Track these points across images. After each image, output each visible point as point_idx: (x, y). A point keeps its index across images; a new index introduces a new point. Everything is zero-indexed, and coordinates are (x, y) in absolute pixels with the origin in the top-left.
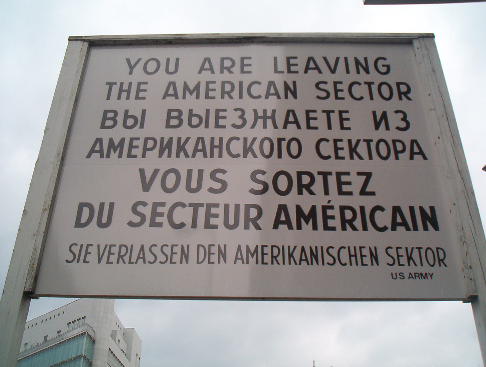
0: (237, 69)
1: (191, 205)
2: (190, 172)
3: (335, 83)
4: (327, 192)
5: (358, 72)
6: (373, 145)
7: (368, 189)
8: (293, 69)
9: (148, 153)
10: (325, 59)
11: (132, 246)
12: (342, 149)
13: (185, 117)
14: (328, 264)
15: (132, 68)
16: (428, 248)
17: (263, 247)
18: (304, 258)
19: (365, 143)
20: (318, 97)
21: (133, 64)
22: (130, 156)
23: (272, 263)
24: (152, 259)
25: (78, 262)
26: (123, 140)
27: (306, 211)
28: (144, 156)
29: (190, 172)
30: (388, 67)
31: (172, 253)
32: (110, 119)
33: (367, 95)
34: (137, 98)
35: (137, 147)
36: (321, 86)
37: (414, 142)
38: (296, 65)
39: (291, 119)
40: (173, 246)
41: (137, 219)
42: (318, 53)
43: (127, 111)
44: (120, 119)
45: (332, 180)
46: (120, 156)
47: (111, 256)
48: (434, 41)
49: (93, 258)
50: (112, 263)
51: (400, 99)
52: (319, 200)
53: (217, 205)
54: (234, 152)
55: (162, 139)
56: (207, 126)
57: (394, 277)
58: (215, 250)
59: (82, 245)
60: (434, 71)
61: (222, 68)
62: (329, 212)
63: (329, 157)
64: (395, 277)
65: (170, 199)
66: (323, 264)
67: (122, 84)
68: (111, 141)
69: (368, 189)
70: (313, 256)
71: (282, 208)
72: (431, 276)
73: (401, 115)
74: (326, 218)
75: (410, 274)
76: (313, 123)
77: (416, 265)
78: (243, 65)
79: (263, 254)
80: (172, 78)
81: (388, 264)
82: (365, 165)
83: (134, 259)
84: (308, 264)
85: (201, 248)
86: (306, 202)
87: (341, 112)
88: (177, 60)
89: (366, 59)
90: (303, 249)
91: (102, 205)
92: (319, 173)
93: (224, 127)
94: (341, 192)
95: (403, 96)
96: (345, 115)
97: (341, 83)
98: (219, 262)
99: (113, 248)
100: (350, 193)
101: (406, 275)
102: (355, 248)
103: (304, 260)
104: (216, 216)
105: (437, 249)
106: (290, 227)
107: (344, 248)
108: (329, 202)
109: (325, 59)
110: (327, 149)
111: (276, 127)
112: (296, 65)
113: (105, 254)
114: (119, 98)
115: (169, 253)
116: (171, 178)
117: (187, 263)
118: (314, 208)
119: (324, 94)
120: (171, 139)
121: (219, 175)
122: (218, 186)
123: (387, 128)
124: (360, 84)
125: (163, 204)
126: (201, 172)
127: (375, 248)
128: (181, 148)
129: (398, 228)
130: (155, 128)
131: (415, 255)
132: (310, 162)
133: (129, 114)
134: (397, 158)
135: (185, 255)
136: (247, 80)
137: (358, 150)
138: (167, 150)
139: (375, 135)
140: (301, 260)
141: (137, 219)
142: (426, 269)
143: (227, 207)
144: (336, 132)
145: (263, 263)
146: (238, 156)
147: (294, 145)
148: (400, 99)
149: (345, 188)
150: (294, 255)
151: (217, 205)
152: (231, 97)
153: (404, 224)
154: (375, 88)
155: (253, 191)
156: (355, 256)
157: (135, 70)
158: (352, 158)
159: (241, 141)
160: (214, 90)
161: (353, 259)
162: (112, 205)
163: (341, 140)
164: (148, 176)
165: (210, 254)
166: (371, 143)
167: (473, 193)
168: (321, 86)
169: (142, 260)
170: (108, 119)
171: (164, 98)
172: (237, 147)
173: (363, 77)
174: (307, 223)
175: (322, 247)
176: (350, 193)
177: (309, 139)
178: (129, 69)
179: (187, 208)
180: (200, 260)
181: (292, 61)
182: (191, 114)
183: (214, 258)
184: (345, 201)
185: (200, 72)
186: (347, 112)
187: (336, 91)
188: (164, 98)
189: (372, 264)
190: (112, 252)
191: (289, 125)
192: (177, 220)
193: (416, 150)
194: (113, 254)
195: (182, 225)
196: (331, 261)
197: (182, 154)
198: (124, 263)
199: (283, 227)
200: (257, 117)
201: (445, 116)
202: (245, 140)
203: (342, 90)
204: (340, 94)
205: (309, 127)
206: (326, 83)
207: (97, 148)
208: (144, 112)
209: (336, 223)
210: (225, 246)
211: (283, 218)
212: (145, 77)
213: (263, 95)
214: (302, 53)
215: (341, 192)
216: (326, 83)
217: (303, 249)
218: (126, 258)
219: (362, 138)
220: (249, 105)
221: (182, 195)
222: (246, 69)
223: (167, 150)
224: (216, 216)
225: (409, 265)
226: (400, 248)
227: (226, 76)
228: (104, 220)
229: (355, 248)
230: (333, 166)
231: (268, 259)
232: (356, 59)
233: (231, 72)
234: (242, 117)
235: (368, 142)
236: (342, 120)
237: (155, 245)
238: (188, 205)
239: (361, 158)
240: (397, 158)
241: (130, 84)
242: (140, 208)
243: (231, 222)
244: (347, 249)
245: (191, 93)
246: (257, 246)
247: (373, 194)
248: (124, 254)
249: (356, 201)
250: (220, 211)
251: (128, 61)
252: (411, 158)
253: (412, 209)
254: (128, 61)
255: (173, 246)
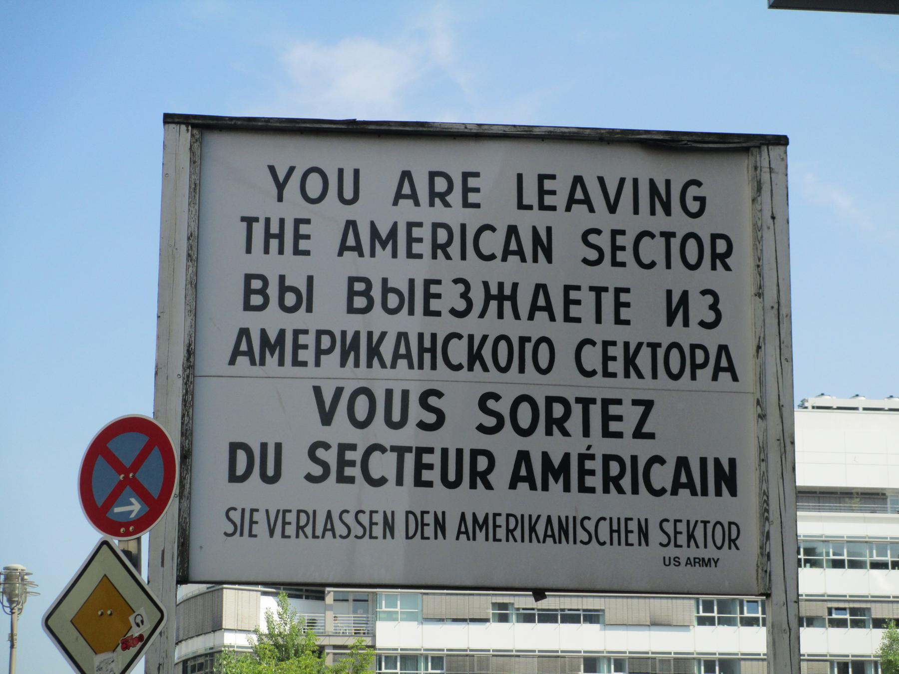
0: (455, 197)
1: (393, 449)
2: (389, 393)
3: (615, 233)
4: (586, 433)
5: (653, 212)
6: (661, 352)
7: (646, 429)
8: (548, 200)
9: (323, 358)
10: (601, 180)
11: (314, 512)
12: (614, 359)
13: (376, 293)
14: (582, 542)
15: (281, 187)
16: (718, 523)
17: (495, 515)
18: (549, 533)
19: (650, 349)
20: (585, 261)
21: (281, 178)
22: (296, 363)
23: (507, 540)
24: (345, 532)
25: (242, 534)
26: (282, 333)
27: (556, 461)
28: (318, 364)
29: (389, 393)
30: (702, 200)
31: (372, 524)
32: (256, 292)
33: (661, 260)
34: (297, 252)
35: (305, 347)
36: (592, 238)
37: (723, 349)
38: (553, 193)
39: (541, 302)
40: (372, 512)
41: (317, 471)
42: (592, 164)
43: (282, 278)
44: (273, 291)
45: (596, 411)
46: (281, 363)
47: (287, 527)
48: (786, 153)
49: (261, 528)
50: (289, 537)
51: (714, 268)
52: (575, 445)
53: (430, 451)
54: (455, 362)
55: (344, 333)
56: (411, 312)
57: (667, 562)
58: (429, 519)
59: (243, 510)
60: (773, 218)
61: (433, 195)
62: (589, 465)
63: (593, 373)
64: (667, 563)
65: (362, 439)
66: (575, 542)
67: (268, 221)
68: (263, 332)
69: (646, 429)
70: (562, 531)
71: (523, 457)
72: (716, 563)
73: (709, 299)
74: (584, 473)
75: (689, 559)
76: (574, 311)
77: (697, 547)
78: (466, 190)
79: (495, 526)
80: (350, 213)
81: (661, 544)
82: (643, 388)
83: (319, 532)
84: (555, 542)
85: (411, 516)
86: (557, 447)
87: (618, 291)
88: (357, 172)
89: (668, 183)
90: (549, 518)
91: (264, 446)
92: (578, 400)
93: (438, 314)
94: (606, 433)
95: (718, 262)
96: (624, 297)
97: (623, 233)
98: (436, 538)
99: (287, 514)
100: (619, 435)
101: (683, 561)
102: (619, 519)
103: (549, 536)
104: (430, 467)
105: (730, 523)
106: (533, 487)
107: (604, 519)
108: (589, 448)
109: (601, 180)
110: (592, 358)
111: (517, 317)
112: (553, 193)
113: (278, 523)
114: (267, 251)
115: (367, 524)
116: (362, 403)
117: (393, 537)
118: (567, 456)
119: (593, 255)
120: (357, 334)
121: (433, 401)
122: (431, 418)
123: (686, 324)
124: (652, 236)
125: (353, 447)
126: (405, 394)
127: (646, 520)
128: (374, 352)
129: (681, 491)
130: (330, 313)
131: (699, 534)
132: (565, 381)
133: (288, 283)
134: (693, 377)
135: (389, 526)
136: (473, 220)
137: (639, 361)
138: (352, 354)
139: (666, 335)
140: (546, 536)
141: (317, 471)
142: (710, 552)
143: (445, 452)
144: (608, 330)
145: (495, 539)
146: (459, 367)
147: (544, 347)
148: (714, 268)
149: (614, 426)
150: (537, 528)
151: (430, 451)
152: (448, 257)
153: (690, 485)
154: (675, 243)
155: (481, 428)
156: (618, 531)
157: (285, 192)
158: (627, 375)
159: (465, 341)
160: (420, 240)
161: (615, 535)
162: (278, 447)
163: (614, 343)
164: (328, 399)
165: (423, 525)
166: (659, 350)
167: (793, 443)
168: (592, 238)
169: (330, 533)
170: (254, 290)
171: (340, 254)
172: (458, 352)
173: (659, 222)
174: (556, 481)
175: (574, 518)
176: (619, 435)
177: (565, 337)
178: (275, 191)
179: (388, 453)
180: (411, 534)
181: (548, 185)
182: (386, 289)
183: (429, 531)
184: (611, 446)
185: (395, 203)
186: (627, 290)
187: (615, 248)
188: (340, 254)
189: (640, 544)
190: (287, 520)
191: (537, 313)
192: (375, 474)
193: (724, 363)
194: (289, 523)
195: (382, 481)
196: (586, 539)
197: (376, 361)
198: (306, 537)
199: (523, 486)
200: (488, 297)
201: (776, 306)
202: (471, 338)
203: (623, 248)
204: (621, 256)
205: (568, 318)
206: (598, 232)
207: (244, 347)
208: (310, 279)
209: (594, 481)
210: (444, 513)
211: (523, 472)
212: (304, 210)
213: (499, 255)
214: (565, 164)
215: (606, 433)
216: (598, 232)
217: (549, 518)
218: (309, 530)
219: (646, 341)
220: (475, 271)
221: (379, 432)
222: (472, 198)
223: (352, 354)
224: (430, 467)
225: (689, 546)
226: (680, 521)
227: (439, 213)
228: (270, 472)
229: (619, 519)
230: (599, 388)
231: (501, 533)
232: (652, 182)
233: (447, 205)
234: (465, 296)
235: (654, 346)
236: (619, 305)
237: (347, 512)
238: (388, 448)
239: (640, 376)
240: (693, 377)
241: (282, 221)
242: (320, 453)
243: (452, 477)
244: (608, 521)
245: (384, 245)
246: (487, 514)
247: (651, 436)
248: (305, 524)
249: (626, 447)
250: (434, 459)
251: (272, 169)
252: (715, 378)
253: (703, 461)
254: (272, 169)
255: (372, 512)
